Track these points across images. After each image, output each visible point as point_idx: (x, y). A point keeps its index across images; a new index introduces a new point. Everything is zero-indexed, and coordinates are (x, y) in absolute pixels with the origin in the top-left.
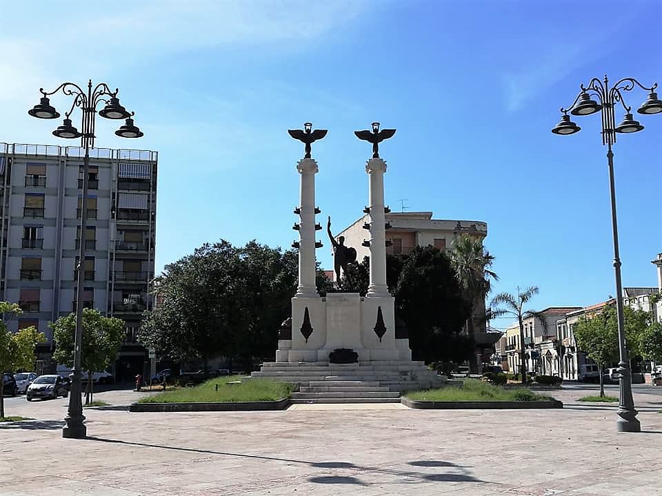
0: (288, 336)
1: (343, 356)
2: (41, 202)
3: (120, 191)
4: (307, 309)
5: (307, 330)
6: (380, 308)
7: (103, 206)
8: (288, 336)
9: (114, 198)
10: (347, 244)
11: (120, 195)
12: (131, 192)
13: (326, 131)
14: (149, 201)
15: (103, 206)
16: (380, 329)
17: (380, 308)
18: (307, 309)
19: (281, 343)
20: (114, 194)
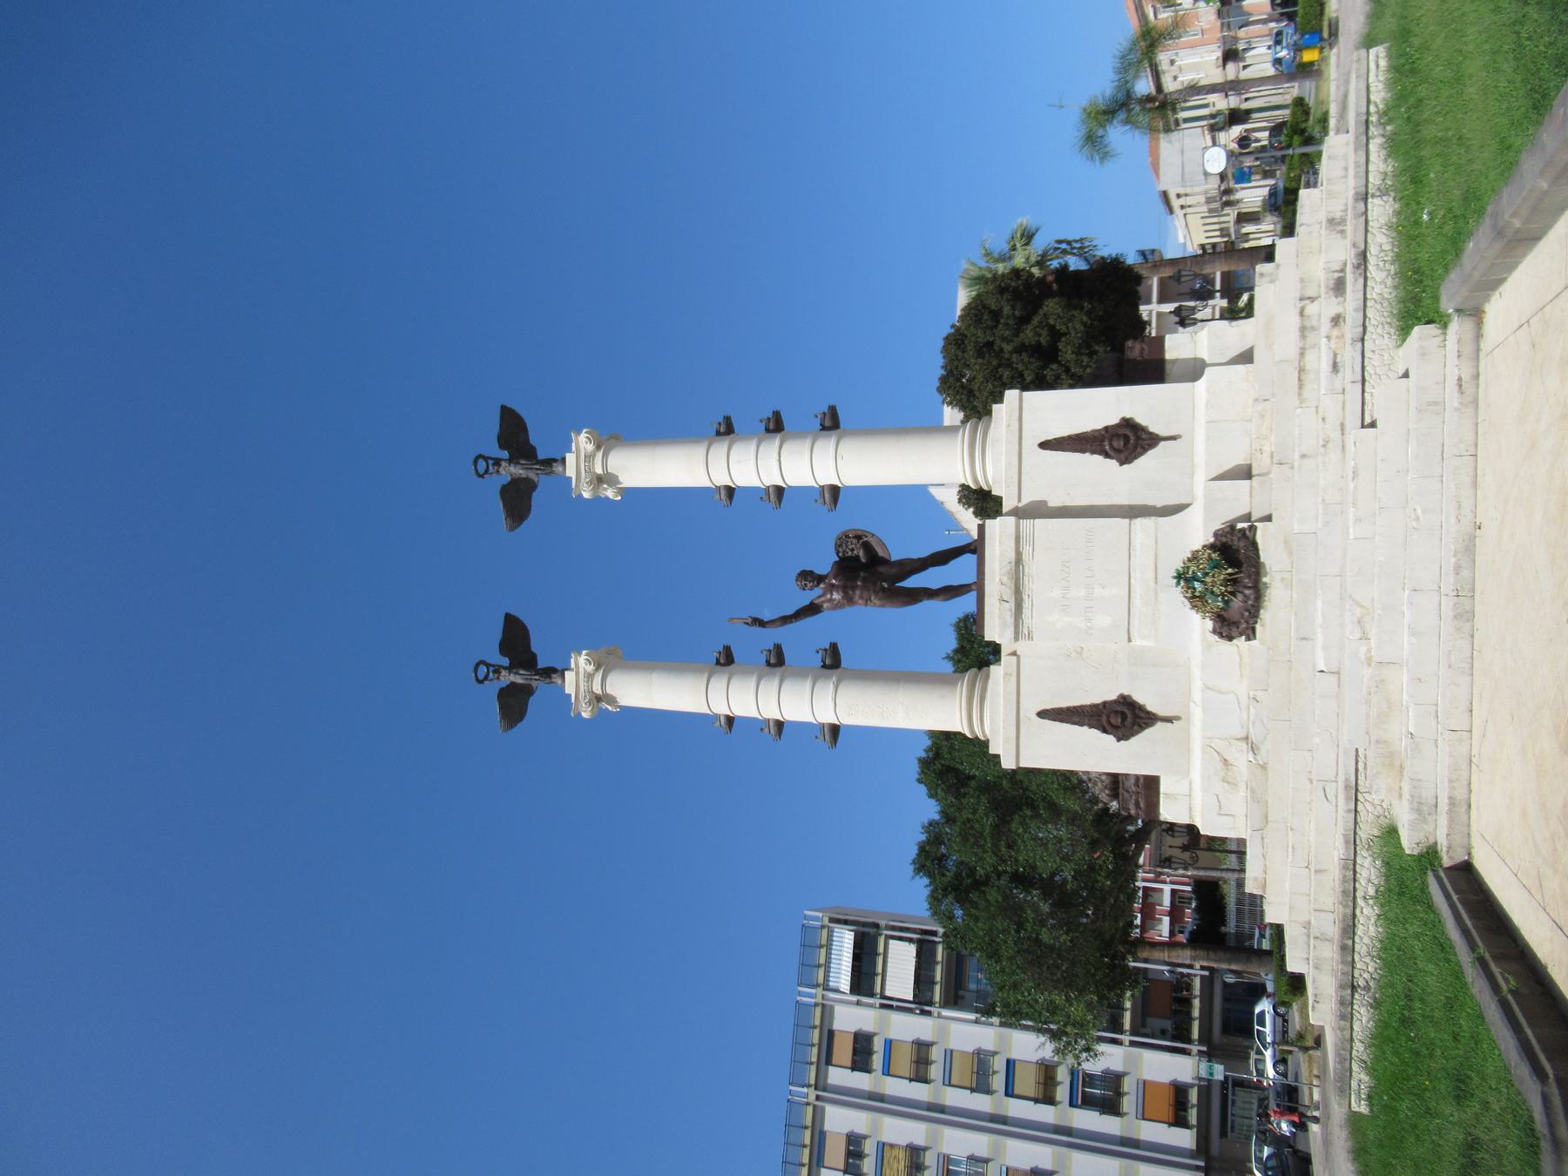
0: (1150, 785)
1: (1229, 578)
2: (895, 1152)
3: (878, 990)
4: (1043, 714)
5: (1123, 717)
6: (1045, 445)
7: (907, 1028)
8: (1150, 785)
9: (890, 1007)
10: (824, 563)
11: (888, 993)
12: (879, 970)
13: (508, 616)
14: (901, 939)
15: (907, 1028)
16: (1126, 441)
17: (1045, 445)
18: (1043, 714)
19: (1169, 812)
20: (883, 1006)
